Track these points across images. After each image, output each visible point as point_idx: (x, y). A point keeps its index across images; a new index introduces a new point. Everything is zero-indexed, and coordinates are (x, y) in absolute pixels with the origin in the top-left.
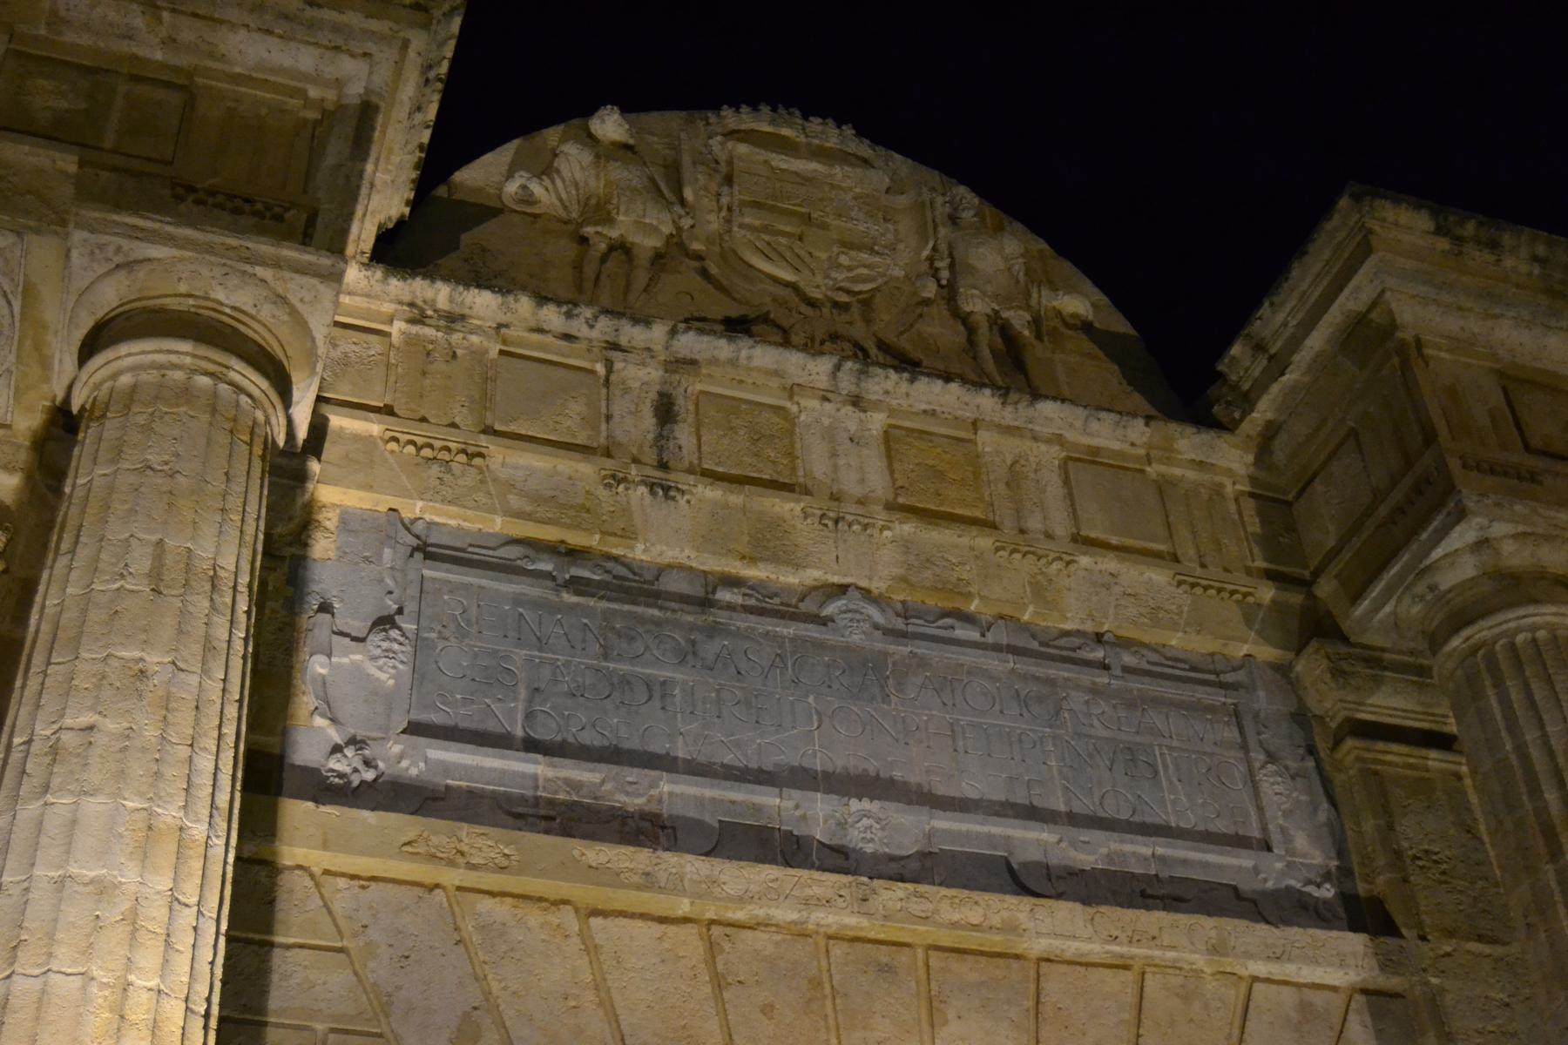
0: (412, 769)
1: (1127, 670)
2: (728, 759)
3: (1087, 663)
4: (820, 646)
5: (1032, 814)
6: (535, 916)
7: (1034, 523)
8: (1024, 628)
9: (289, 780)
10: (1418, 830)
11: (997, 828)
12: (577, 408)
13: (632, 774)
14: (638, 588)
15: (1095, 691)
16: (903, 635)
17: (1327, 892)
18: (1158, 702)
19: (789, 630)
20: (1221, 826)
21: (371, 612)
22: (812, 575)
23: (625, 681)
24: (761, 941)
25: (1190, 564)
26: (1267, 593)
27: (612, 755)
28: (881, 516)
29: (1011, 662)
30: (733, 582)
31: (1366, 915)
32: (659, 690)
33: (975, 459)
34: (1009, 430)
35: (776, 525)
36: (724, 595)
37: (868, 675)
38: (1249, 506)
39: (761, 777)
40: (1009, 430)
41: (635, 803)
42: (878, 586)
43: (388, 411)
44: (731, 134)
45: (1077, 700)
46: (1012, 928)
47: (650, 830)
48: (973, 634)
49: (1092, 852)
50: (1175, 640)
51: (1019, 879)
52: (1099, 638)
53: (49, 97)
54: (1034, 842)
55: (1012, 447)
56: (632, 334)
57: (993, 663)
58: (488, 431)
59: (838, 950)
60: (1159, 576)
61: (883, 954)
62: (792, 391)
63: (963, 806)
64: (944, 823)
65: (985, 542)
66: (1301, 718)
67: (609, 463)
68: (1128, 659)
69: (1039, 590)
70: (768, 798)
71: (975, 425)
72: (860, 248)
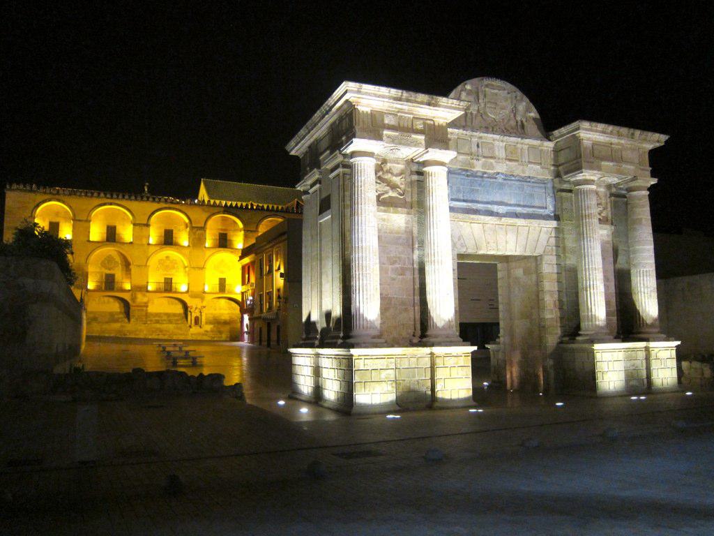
1: (533, 182)
2: (485, 200)
5: (519, 206)
6: (465, 224)
7: (524, 160)
8: (521, 177)
10: (566, 205)
11: (515, 208)
12: (468, 147)
13: (475, 204)
14: (474, 175)
16: (505, 180)
17: (552, 214)
19: (492, 180)
20: (541, 205)
26: (552, 168)
27: (472, 201)
29: (517, 183)
30: (485, 173)
31: (557, 218)
33: (517, 149)
35: (491, 163)
36: (485, 175)
37: (501, 186)
38: (552, 152)
39: (488, 203)
40: (522, 144)
42: (503, 172)
45: (525, 187)
47: (476, 212)
48: (513, 178)
51: (517, 215)
52: (529, 177)
53: (419, 126)
54: (519, 210)
56: (475, 134)
60: (539, 167)
61: (501, 226)
62: (494, 140)
63: (510, 205)
64: (509, 208)
65: (516, 163)
66: (553, 187)
69: (523, 171)
70: (489, 206)
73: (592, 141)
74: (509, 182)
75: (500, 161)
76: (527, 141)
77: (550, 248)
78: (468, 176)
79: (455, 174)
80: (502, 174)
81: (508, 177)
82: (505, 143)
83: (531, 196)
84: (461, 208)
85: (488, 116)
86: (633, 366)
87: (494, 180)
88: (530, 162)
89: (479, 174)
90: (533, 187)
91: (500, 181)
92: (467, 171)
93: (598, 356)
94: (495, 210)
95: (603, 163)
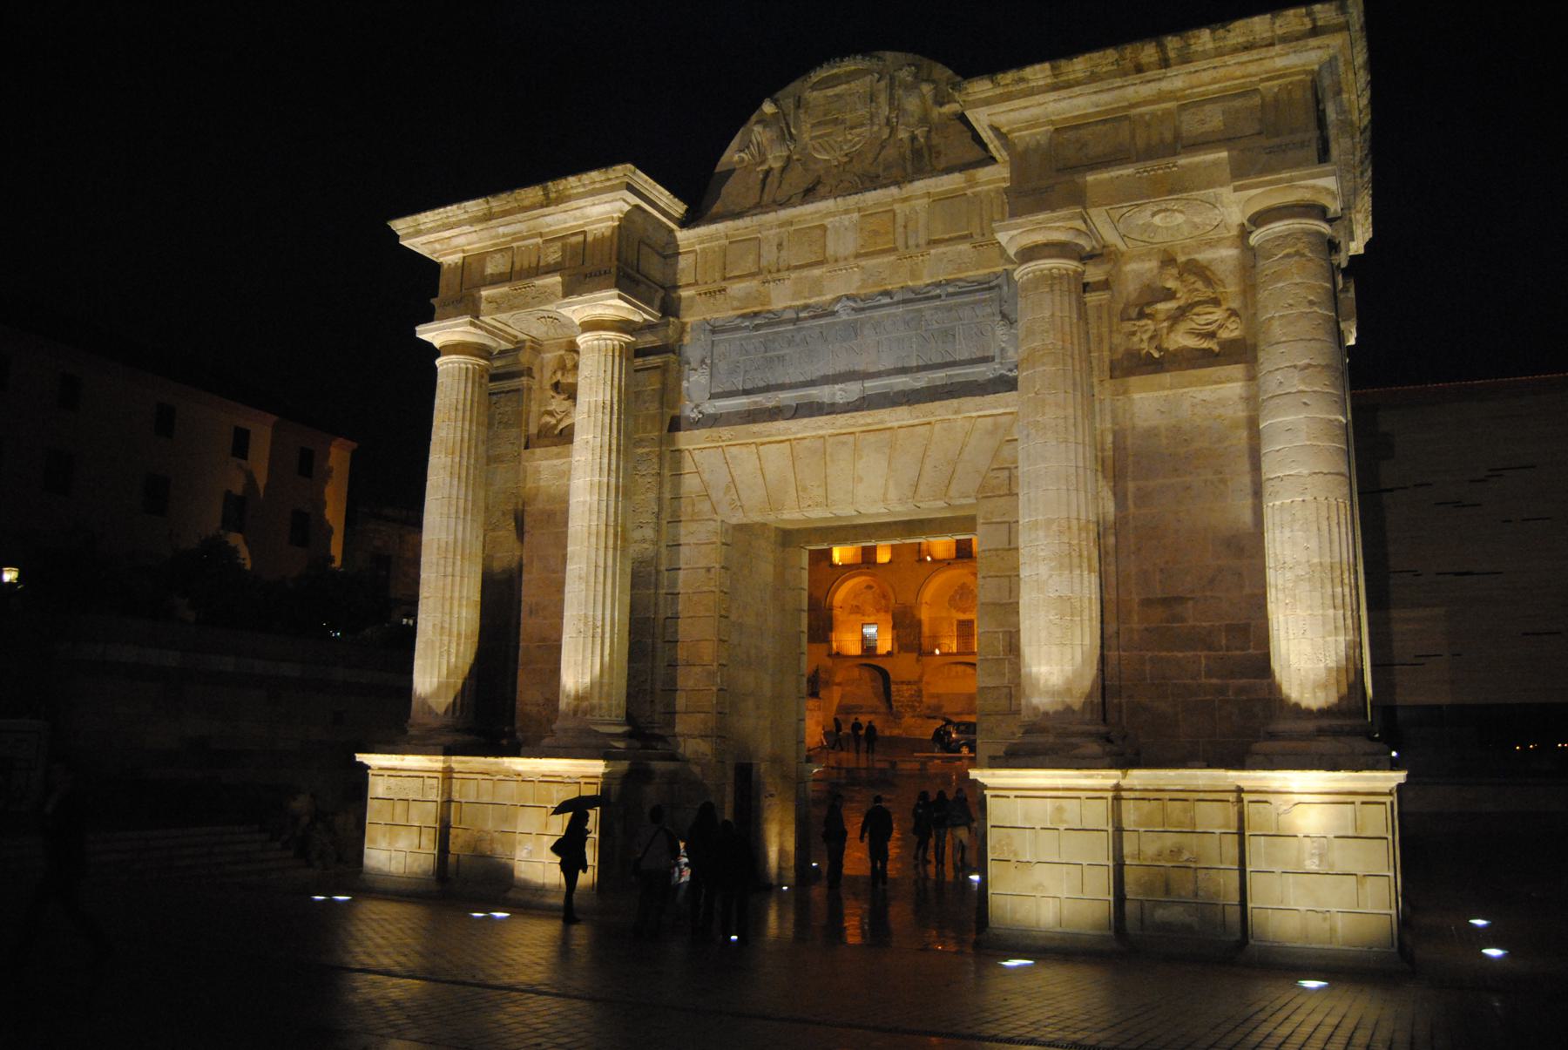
0: (711, 411)
1: (949, 295)
2: (802, 379)
3: (933, 298)
4: (834, 324)
5: (904, 371)
6: (744, 449)
9: (683, 423)
12: (751, 258)
13: (769, 395)
14: (775, 319)
15: (936, 308)
18: (960, 305)
19: (823, 321)
20: (979, 354)
21: (699, 358)
22: (829, 297)
23: (771, 360)
24: (806, 442)
25: (978, 238)
27: (768, 389)
28: (852, 262)
29: (900, 309)
30: (806, 307)
32: (781, 358)
34: (905, 200)
36: (802, 315)
37: (853, 329)
40: (905, 200)
41: (770, 405)
43: (696, 283)
44: (814, 88)
45: (927, 314)
46: (881, 422)
47: (775, 414)
48: (887, 300)
49: (921, 381)
50: (972, 274)
55: (906, 207)
57: (893, 310)
58: (725, 279)
59: (831, 440)
60: (964, 247)
64: (868, 384)
65: (893, 258)
67: (761, 277)
68: (950, 290)
71: (895, 201)
72: (852, 128)
73: (1052, 123)
74: (876, 314)
75: (841, 264)
76: (920, 186)
77: (1006, 473)
78: (757, 327)
79: (723, 331)
80: (848, 297)
81: (862, 303)
82: (856, 216)
83: (948, 334)
84: (738, 413)
85: (816, 161)
86: (1176, 852)
87: (829, 320)
88: (933, 243)
89: (791, 315)
90: (950, 309)
91: (845, 317)
92: (756, 314)
93: (997, 810)
94: (827, 400)
95: (1090, 178)
